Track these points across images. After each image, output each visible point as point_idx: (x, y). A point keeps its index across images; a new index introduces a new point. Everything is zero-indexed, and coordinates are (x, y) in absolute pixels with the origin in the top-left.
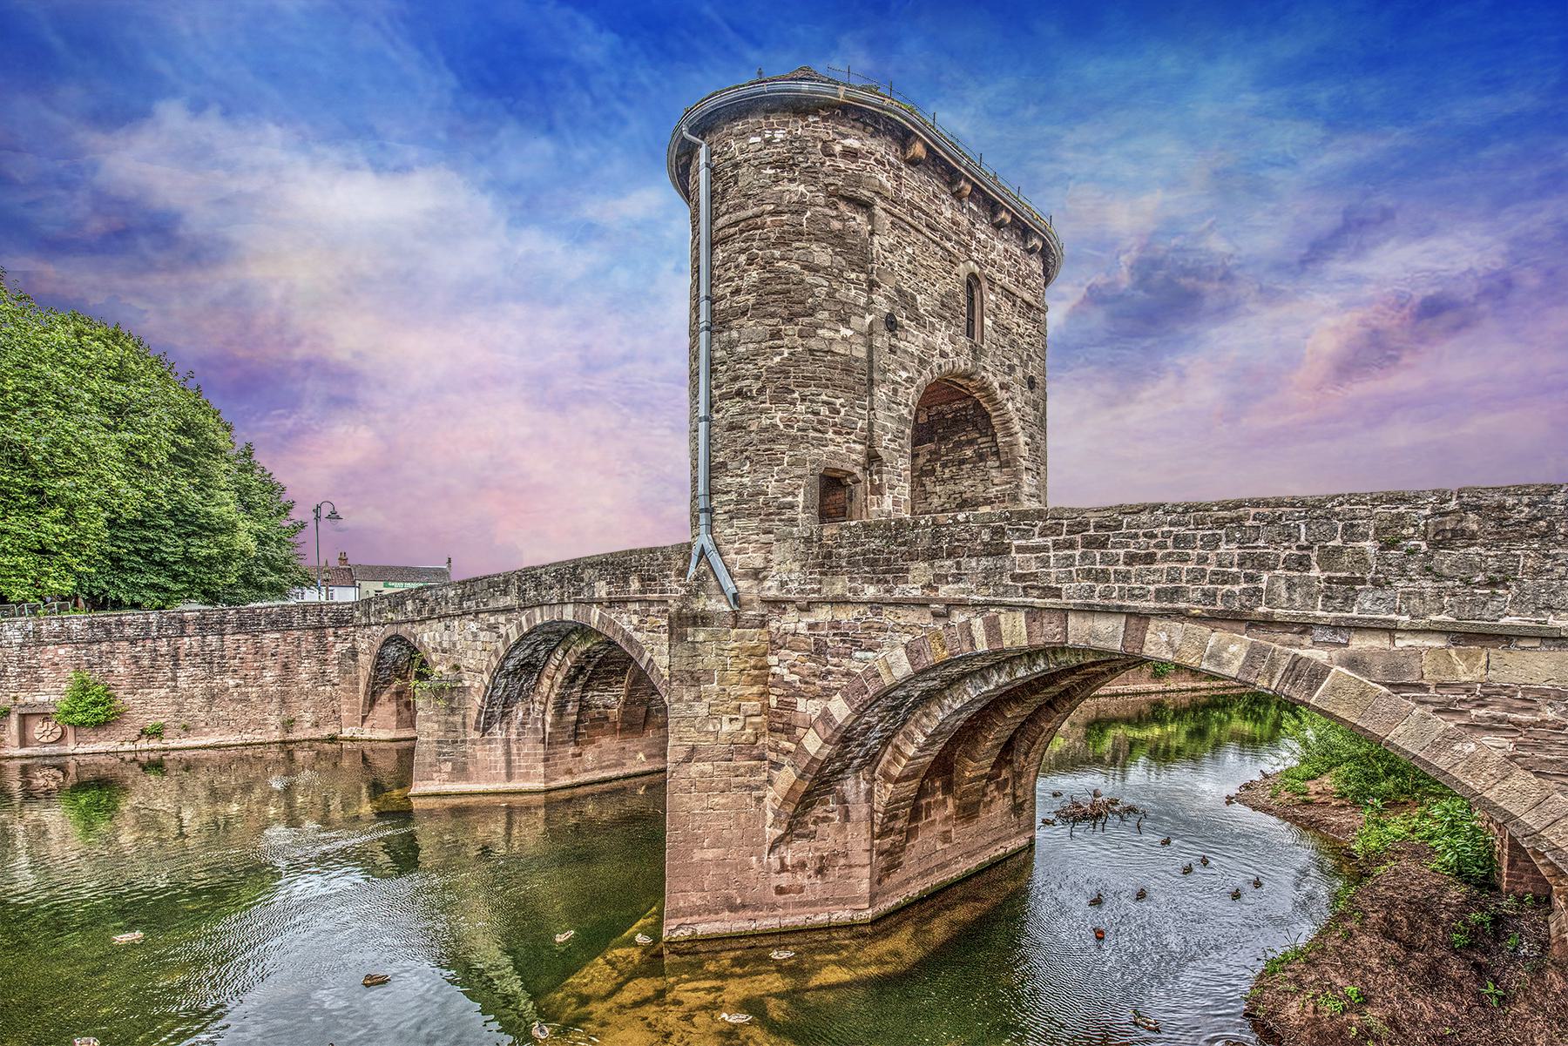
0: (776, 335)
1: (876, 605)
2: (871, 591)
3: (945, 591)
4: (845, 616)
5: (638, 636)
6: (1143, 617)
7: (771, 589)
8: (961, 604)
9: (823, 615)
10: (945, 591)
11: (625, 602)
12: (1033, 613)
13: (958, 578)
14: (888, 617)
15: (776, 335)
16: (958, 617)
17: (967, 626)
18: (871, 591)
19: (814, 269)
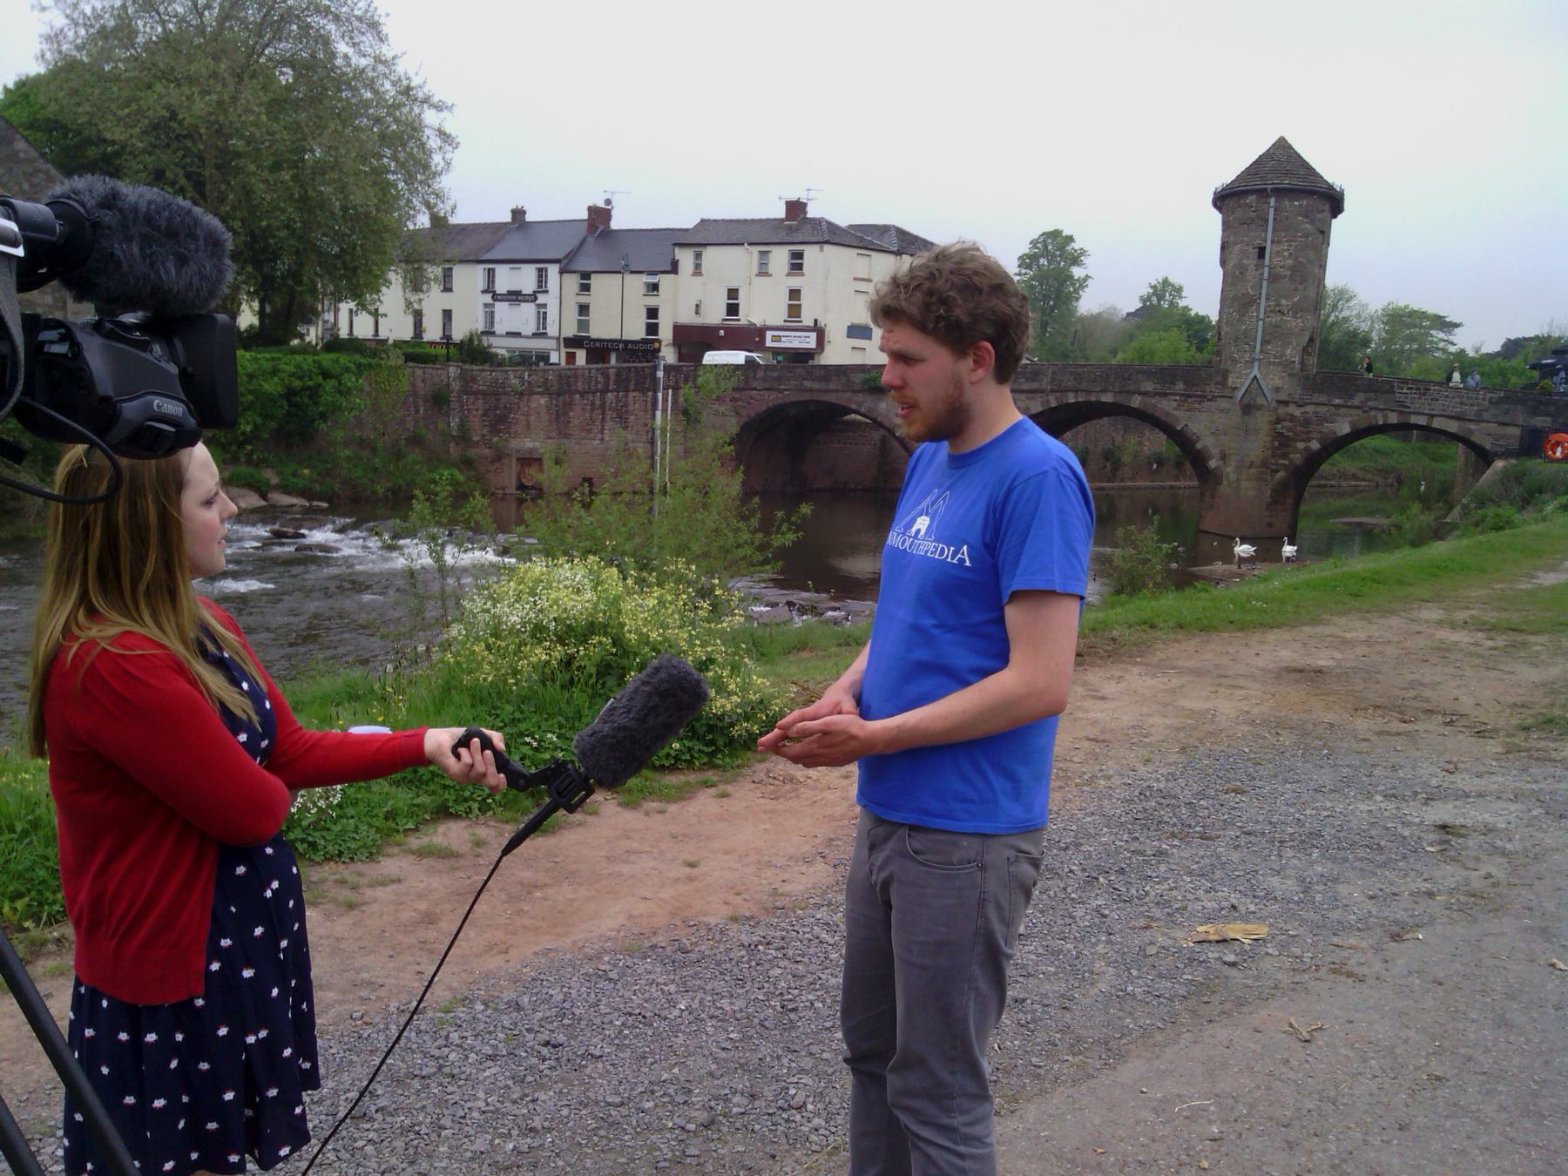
0: (1296, 290)
1: (1338, 406)
2: (1337, 401)
3: (1369, 403)
4: (1322, 409)
5: (1177, 413)
6: (1433, 416)
7: (1283, 396)
8: (1375, 409)
9: (1310, 409)
10: (1369, 403)
11: (1166, 395)
12: (1400, 412)
13: (1376, 400)
14: (1342, 411)
15: (1296, 290)
16: (1373, 413)
17: (1376, 416)
18: (1337, 401)
19: (1309, 261)
